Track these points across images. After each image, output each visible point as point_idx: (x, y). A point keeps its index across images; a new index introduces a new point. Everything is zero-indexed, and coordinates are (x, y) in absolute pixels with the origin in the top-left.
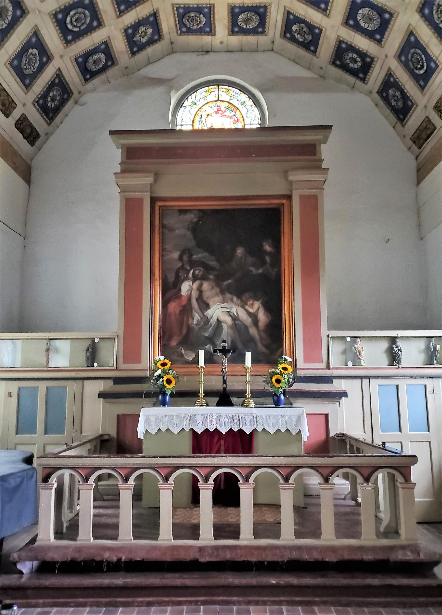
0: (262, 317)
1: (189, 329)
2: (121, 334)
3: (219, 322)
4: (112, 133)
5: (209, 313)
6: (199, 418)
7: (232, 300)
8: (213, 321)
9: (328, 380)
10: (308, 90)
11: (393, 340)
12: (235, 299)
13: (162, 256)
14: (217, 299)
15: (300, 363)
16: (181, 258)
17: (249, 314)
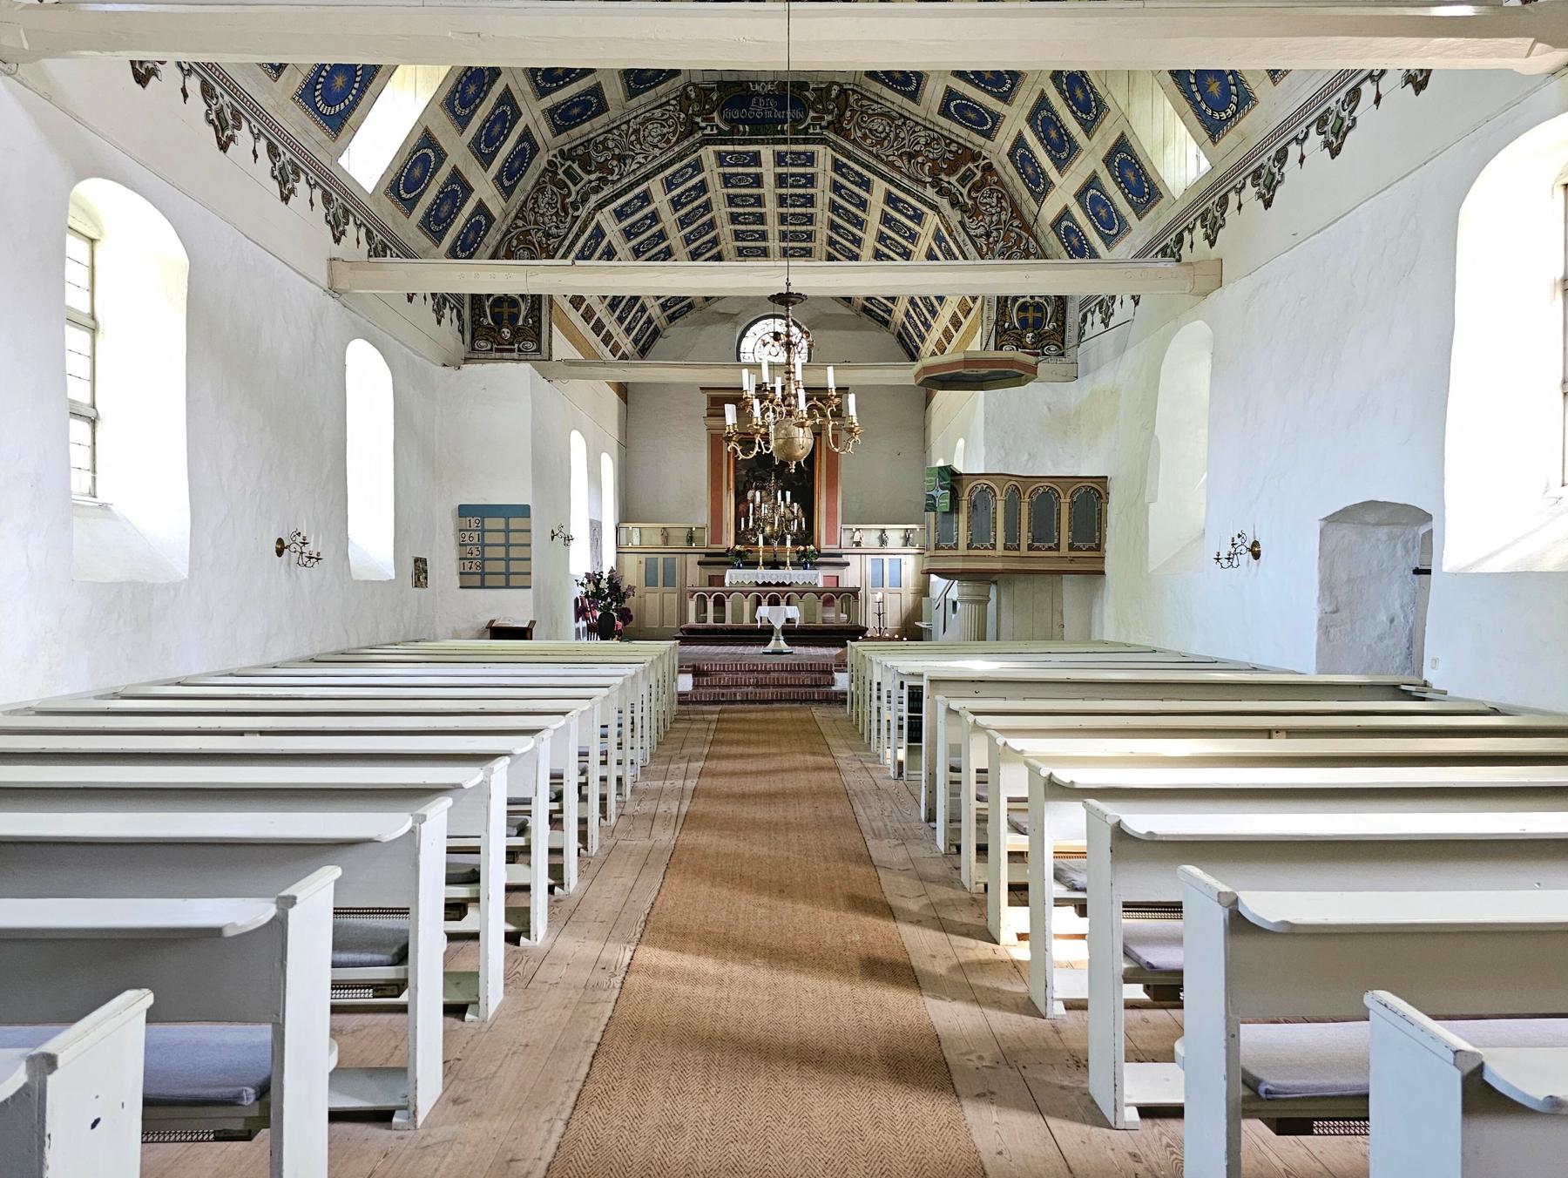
2: (709, 525)
4: (701, 389)
6: (760, 576)
9: (840, 555)
10: (845, 328)
11: (883, 531)
13: (735, 472)
15: (823, 545)
16: (747, 473)
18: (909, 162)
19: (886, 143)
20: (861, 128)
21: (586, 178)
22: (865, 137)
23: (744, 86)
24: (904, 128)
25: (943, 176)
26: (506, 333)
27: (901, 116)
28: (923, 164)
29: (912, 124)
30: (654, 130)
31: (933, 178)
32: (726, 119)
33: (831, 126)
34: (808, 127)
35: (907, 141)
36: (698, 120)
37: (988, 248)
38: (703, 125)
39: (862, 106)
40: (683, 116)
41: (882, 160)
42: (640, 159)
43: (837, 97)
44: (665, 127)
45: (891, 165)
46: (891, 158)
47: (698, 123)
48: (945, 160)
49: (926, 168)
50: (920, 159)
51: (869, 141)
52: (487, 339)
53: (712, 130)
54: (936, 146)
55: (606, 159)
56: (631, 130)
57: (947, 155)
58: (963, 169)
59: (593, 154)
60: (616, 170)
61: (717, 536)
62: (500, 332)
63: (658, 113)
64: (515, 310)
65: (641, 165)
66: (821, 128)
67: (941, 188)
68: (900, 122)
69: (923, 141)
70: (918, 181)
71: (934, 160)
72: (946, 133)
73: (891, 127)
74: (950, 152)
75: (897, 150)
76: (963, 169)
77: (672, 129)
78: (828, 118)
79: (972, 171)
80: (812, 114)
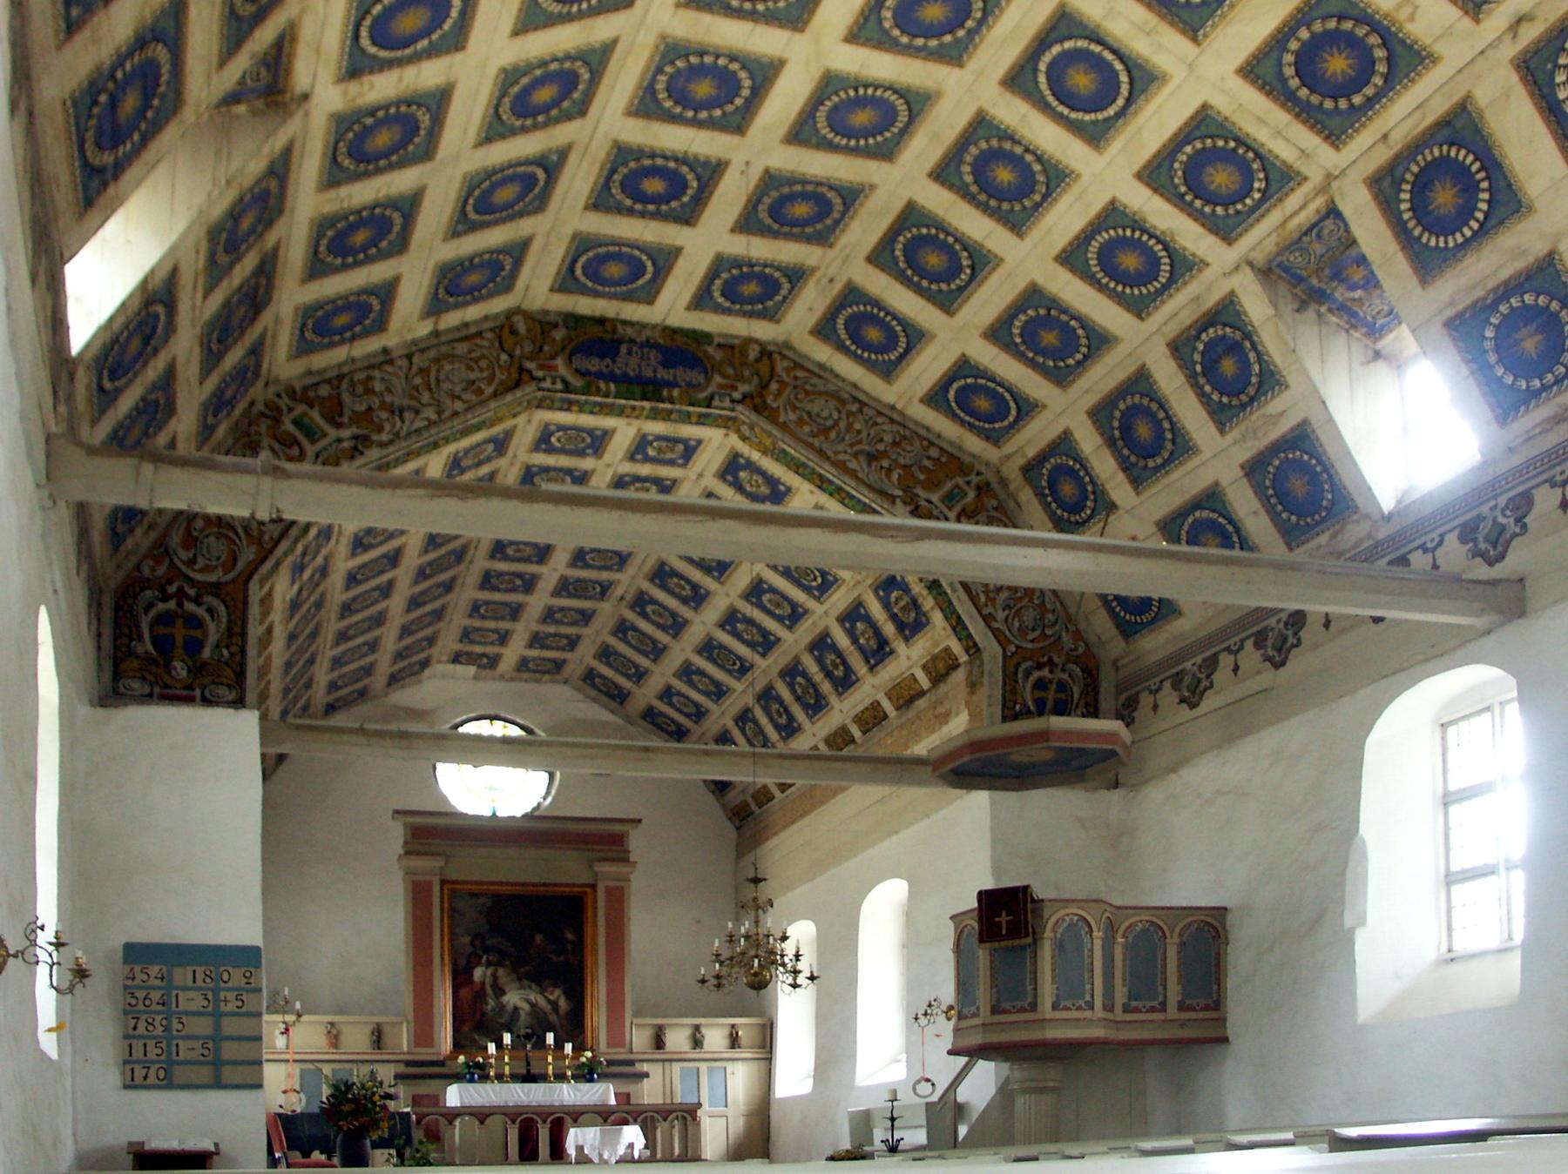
0: (563, 1004)
1: (483, 1015)
3: (516, 1009)
5: (505, 999)
7: (530, 987)
8: (510, 1007)
12: (533, 985)
14: (513, 985)
17: (549, 1001)
18: (869, 465)
19: (833, 435)
20: (794, 408)
21: (333, 433)
22: (801, 421)
23: (608, 326)
24: (860, 416)
25: (919, 491)
26: (180, 669)
27: (855, 399)
28: (889, 471)
29: (871, 413)
30: (457, 373)
31: (905, 491)
32: (577, 371)
33: (748, 401)
34: (711, 398)
35: (864, 435)
36: (530, 365)
37: (987, 596)
38: (540, 374)
39: (796, 378)
40: (504, 357)
41: (828, 458)
42: (430, 413)
43: (758, 361)
44: (473, 370)
45: (841, 466)
46: (841, 457)
47: (530, 372)
48: (923, 469)
49: (895, 477)
50: (885, 463)
51: (807, 429)
52: (144, 678)
53: (554, 383)
54: (909, 448)
55: (370, 409)
56: (415, 368)
57: (926, 463)
58: (949, 485)
59: (346, 397)
60: (387, 427)
61: (424, 1033)
62: (168, 668)
63: (462, 348)
64: (197, 633)
65: (431, 423)
66: (732, 401)
67: (917, 507)
68: (854, 407)
69: (888, 438)
70: (882, 493)
71: (905, 467)
72: (923, 432)
73: (840, 412)
74: (929, 458)
75: (851, 446)
76: (949, 485)
77: (485, 375)
78: (744, 388)
79: (963, 491)
80: (718, 379)
